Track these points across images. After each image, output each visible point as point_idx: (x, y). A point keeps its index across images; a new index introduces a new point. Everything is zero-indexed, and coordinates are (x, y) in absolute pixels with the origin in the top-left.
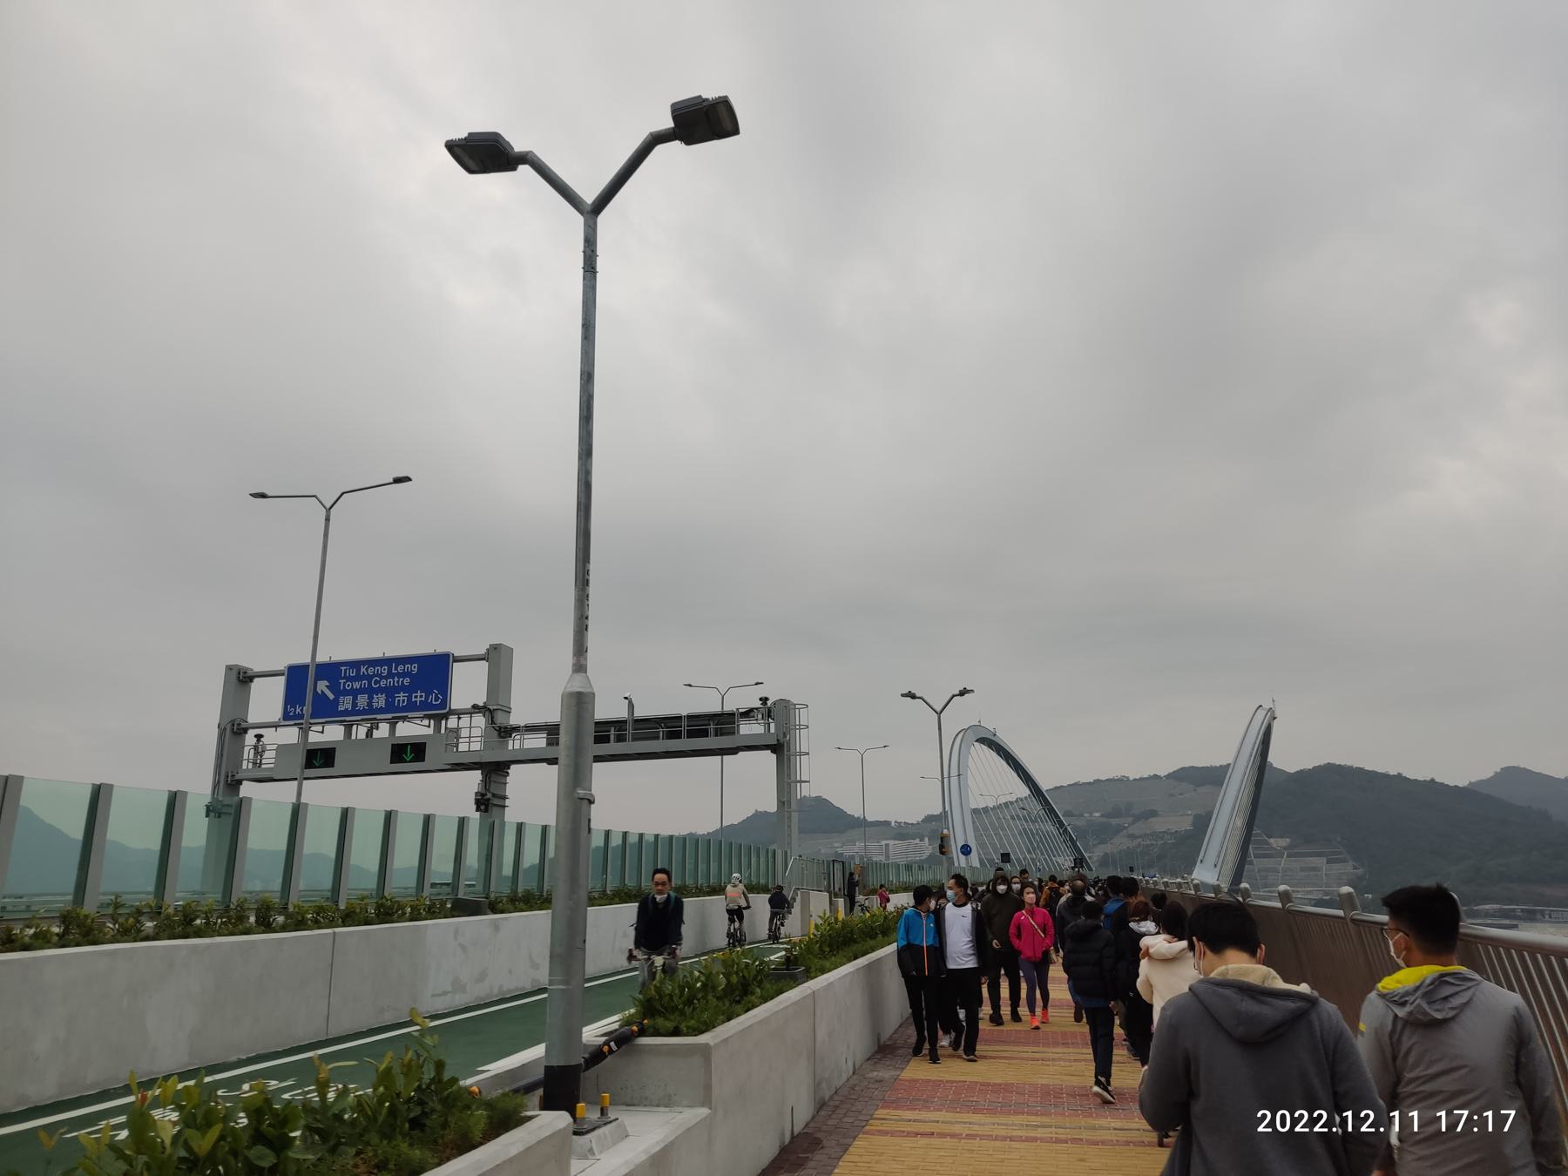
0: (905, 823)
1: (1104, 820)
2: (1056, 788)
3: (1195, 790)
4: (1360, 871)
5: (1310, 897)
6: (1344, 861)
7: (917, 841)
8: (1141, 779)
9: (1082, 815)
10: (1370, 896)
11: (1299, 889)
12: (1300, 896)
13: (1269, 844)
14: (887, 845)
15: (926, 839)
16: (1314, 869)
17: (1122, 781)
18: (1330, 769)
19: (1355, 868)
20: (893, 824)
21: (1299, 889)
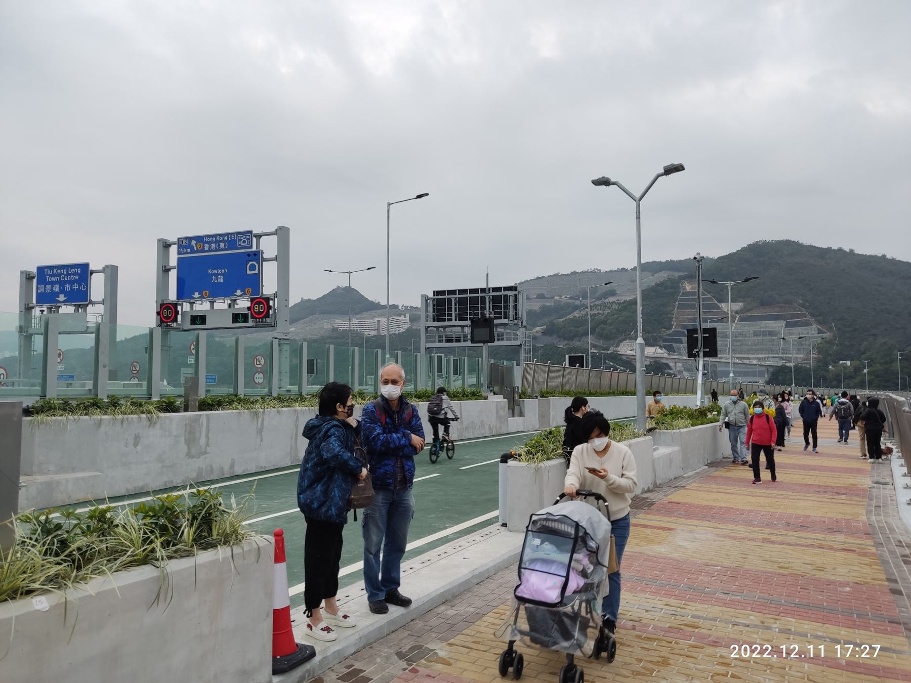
0: (411, 307)
1: (571, 301)
2: (538, 278)
3: (653, 275)
4: (827, 335)
5: (768, 363)
6: (807, 324)
7: (402, 317)
8: (610, 271)
9: (553, 298)
10: (849, 363)
11: (750, 356)
12: (755, 362)
13: (718, 308)
14: (379, 322)
15: (407, 316)
16: (771, 333)
17: (596, 273)
18: (788, 243)
19: (820, 332)
20: (400, 308)
21: (750, 356)
